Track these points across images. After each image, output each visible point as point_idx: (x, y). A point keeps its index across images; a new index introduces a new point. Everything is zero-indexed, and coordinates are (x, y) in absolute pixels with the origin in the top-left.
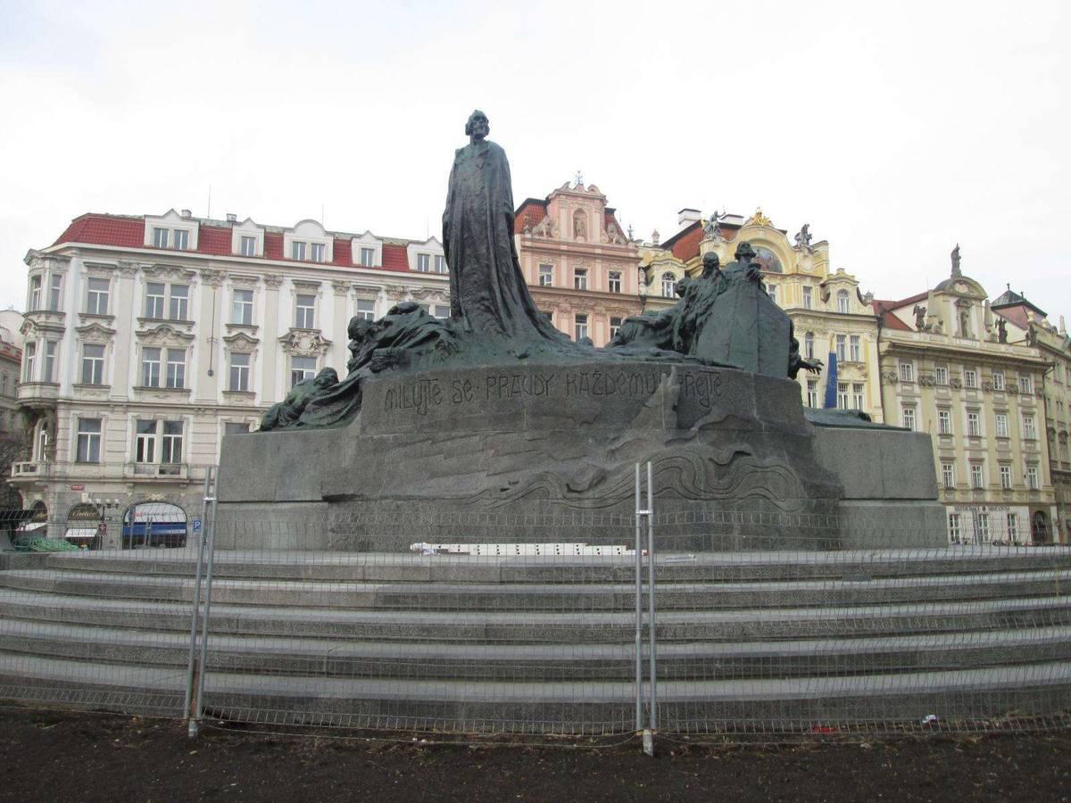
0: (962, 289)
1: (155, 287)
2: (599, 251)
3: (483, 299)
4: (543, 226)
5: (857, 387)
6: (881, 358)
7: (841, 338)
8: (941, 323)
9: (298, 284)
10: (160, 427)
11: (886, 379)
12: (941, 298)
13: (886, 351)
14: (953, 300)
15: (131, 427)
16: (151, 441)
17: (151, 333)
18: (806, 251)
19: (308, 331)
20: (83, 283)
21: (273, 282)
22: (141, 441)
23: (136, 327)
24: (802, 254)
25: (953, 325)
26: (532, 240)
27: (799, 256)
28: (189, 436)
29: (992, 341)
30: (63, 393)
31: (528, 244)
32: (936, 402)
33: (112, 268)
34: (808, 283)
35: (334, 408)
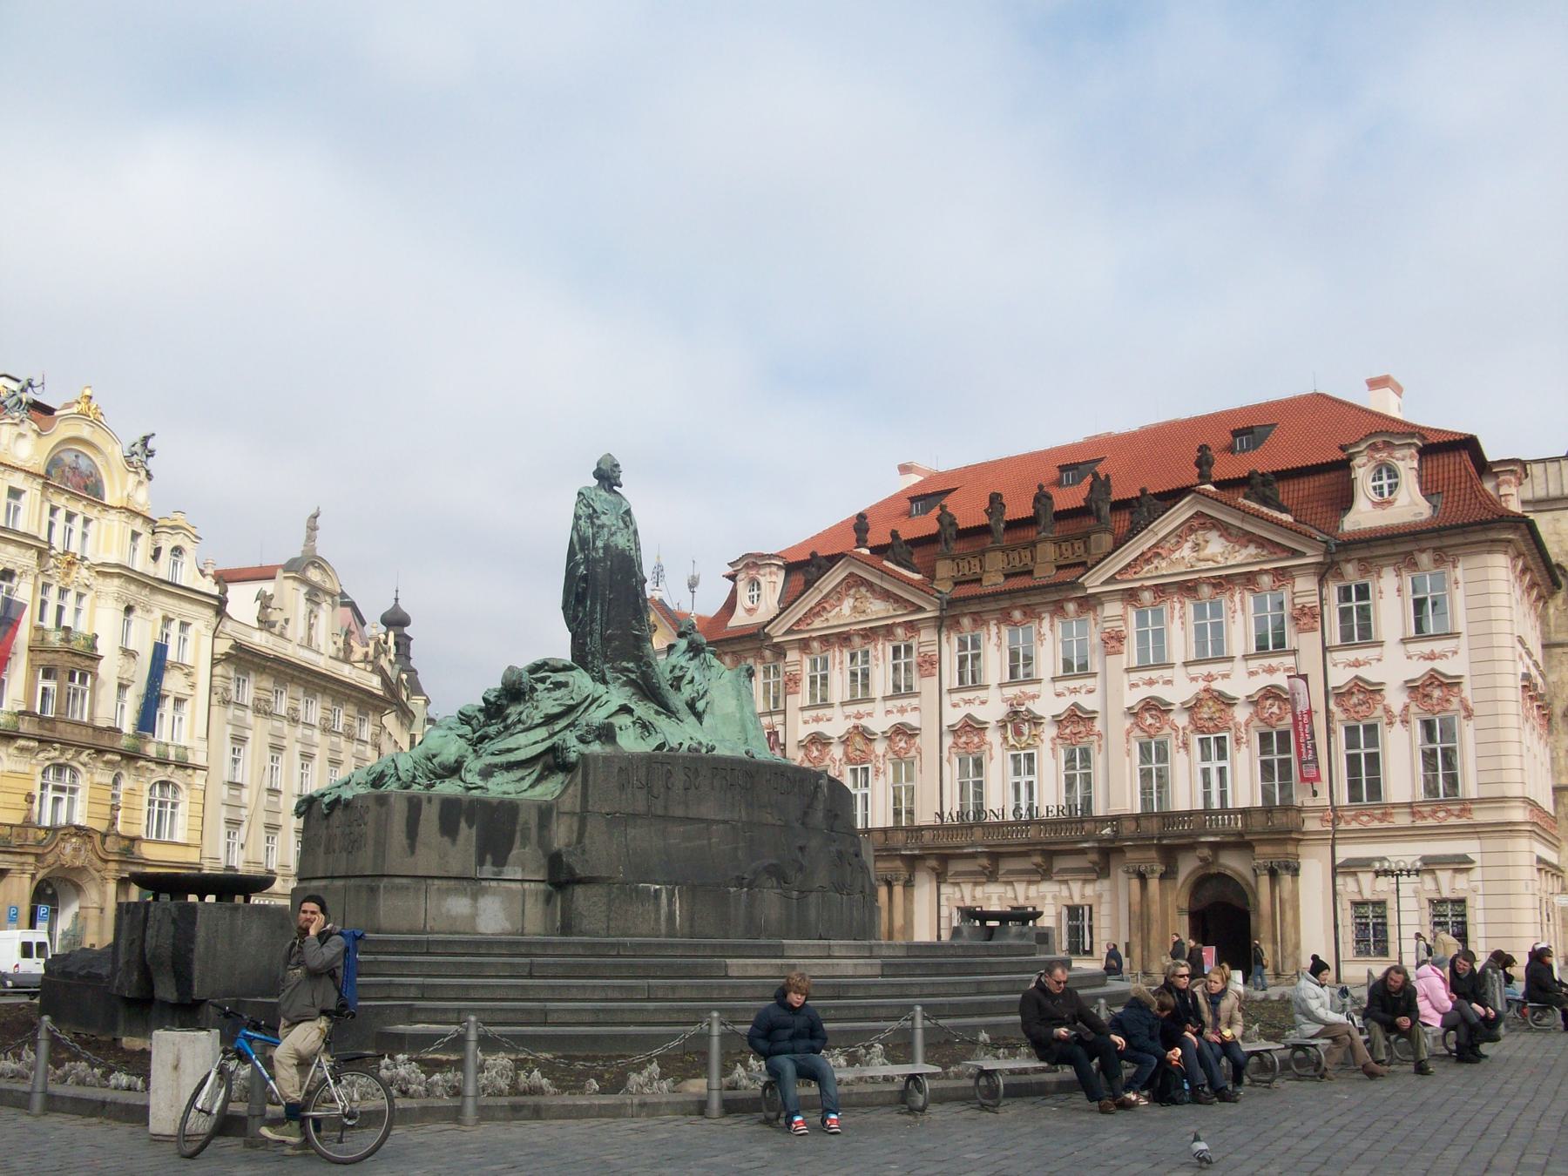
0: (314, 575)
3: (628, 670)
5: (179, 701)
6: (215, 662)
7: (167, 620)
8: (287, 621)
12: (290, 584)
13: (227, 654)
14: (304, 590)
18: (143, 473)
24: (136, 478)
25: (297, 630)
27: (132, 479)
29: (336, 659)
32: (270, 740)
34: (138, 525)
35: (519, 773)
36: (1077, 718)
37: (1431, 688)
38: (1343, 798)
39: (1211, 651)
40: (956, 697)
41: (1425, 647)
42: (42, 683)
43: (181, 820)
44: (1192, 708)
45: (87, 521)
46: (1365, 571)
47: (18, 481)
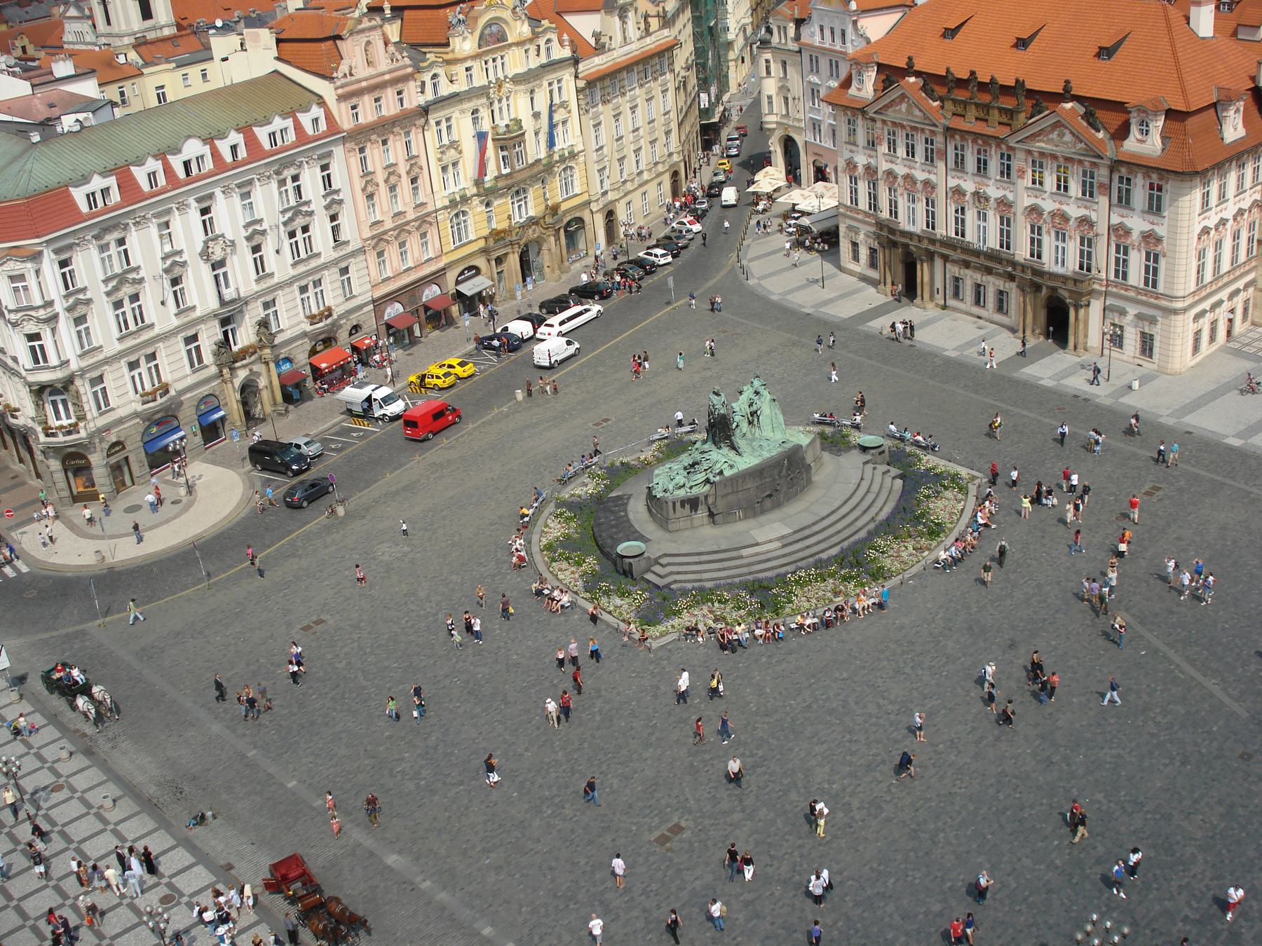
1: (104, 248)
2: (387, 77)
4: (344, 68)
5: (564, 122)
6: (578, 91)
9: (199, 200)
10: (143, 361)
11: (583, 111)
15: (125, 369)
16: (140, 374)
17: (116, 289)
19: (215, 239)
20: (56, 266)
21: (182, 207)
22: (133, 377)
23: (104, 289)
26: (342, 87)
27: (519, 23)
28: (162, 360)
29: (642, 38)
30: (74, 366)
31: (340, 91)
33: (70, 247)
36: (1004, 204)
37: (1150, 238)
38: (1112, 277)
39: (1062, 186)
40: (954, 173)
41: (1152, 218)
42: (501, 154)
43: (576, 183)
44: (1053, 215)
45: (502, 57)
46: (1130, 173)
47: (468, 64)
